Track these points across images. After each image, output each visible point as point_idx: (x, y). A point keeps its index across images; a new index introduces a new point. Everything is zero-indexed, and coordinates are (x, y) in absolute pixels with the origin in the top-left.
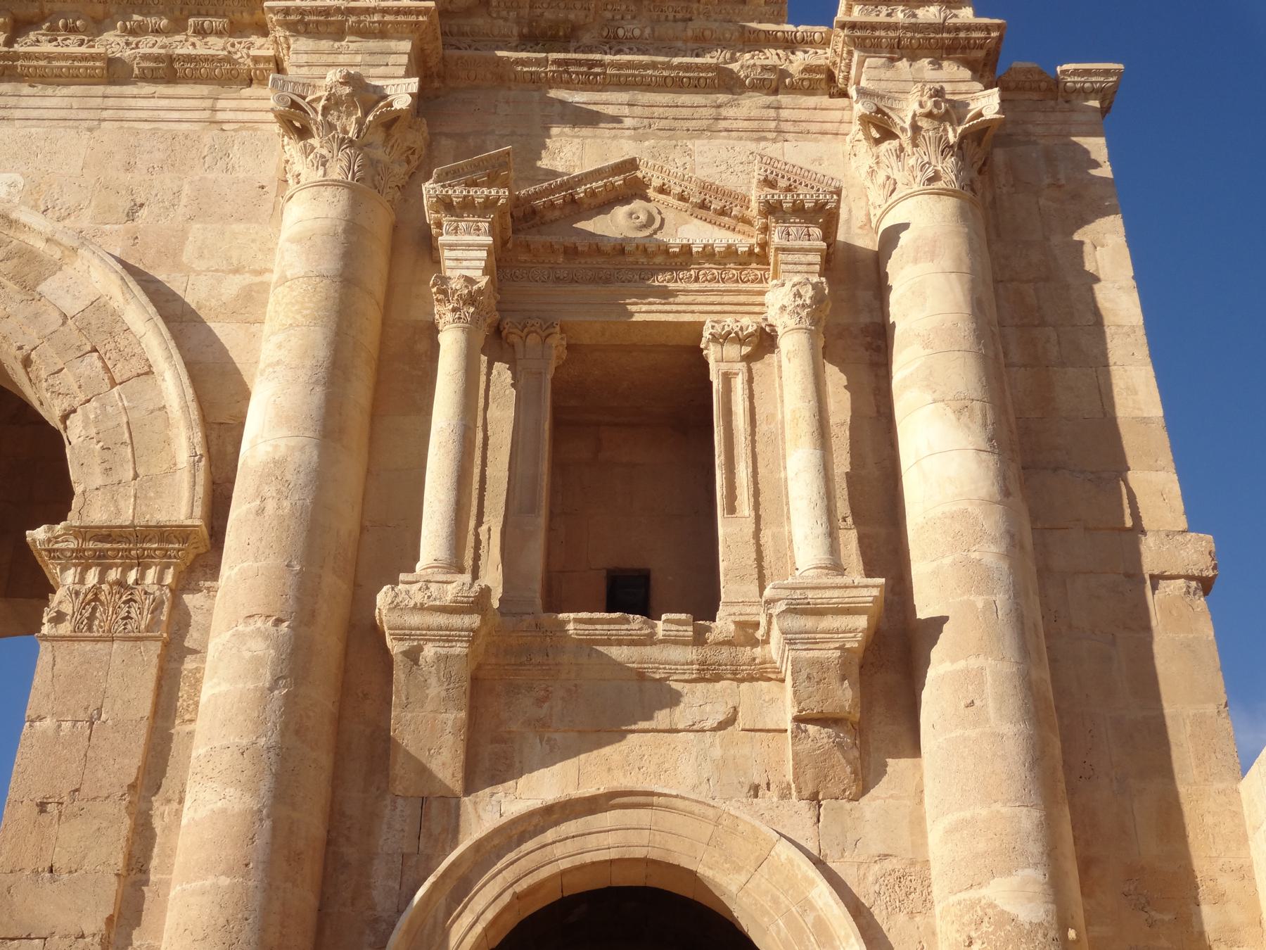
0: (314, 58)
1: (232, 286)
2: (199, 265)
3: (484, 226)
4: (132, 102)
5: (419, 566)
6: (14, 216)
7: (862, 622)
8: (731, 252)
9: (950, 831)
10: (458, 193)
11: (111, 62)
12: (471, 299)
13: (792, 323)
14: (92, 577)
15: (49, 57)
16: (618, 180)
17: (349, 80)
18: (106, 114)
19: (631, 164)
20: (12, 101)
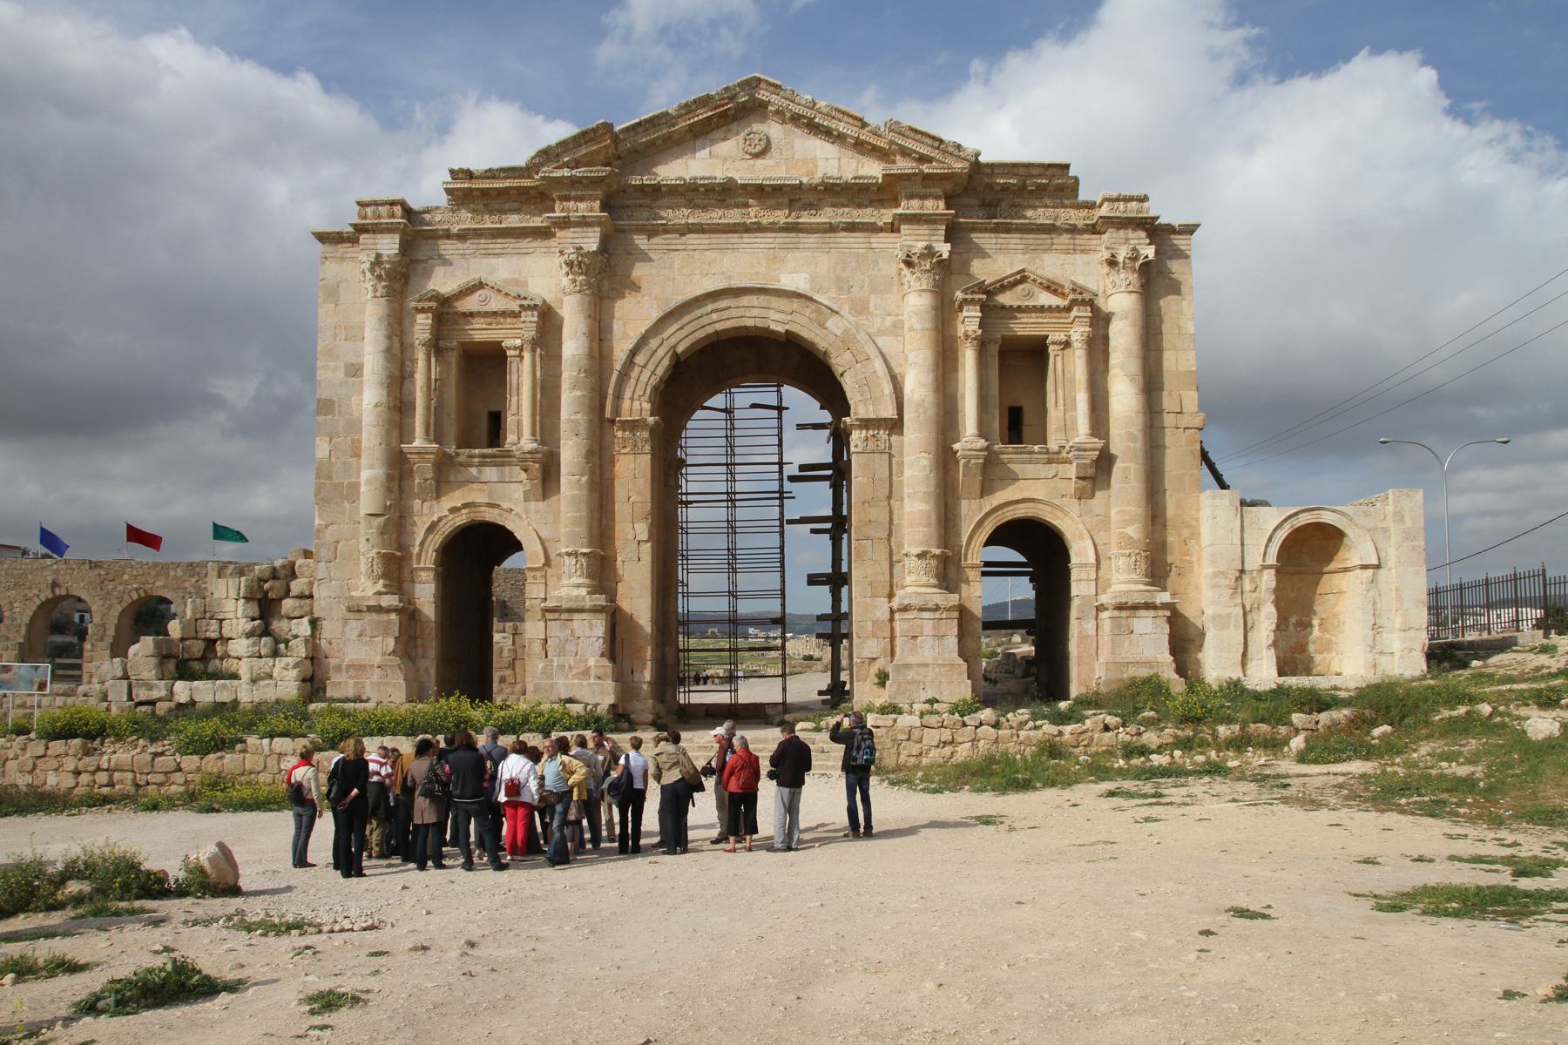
0: (910, 232)
1: (889, 321)
2: (877, 312)
3: (978, 308)
4: (839, 240)
5: (967, 434)
6: (815, 298)
7: (1098, 453)
8: (1058, 306)
9: (1119, 512)
10: (969, 297)
11: (830, 223)
12: (974, 339)
13: (1080, 346)
14: (864, 432)
15: (810, 224)
16: (1018, 277)
17: (929, 248)
18: (832, 245)
19: (1023, 271)
20: (797, 240)
